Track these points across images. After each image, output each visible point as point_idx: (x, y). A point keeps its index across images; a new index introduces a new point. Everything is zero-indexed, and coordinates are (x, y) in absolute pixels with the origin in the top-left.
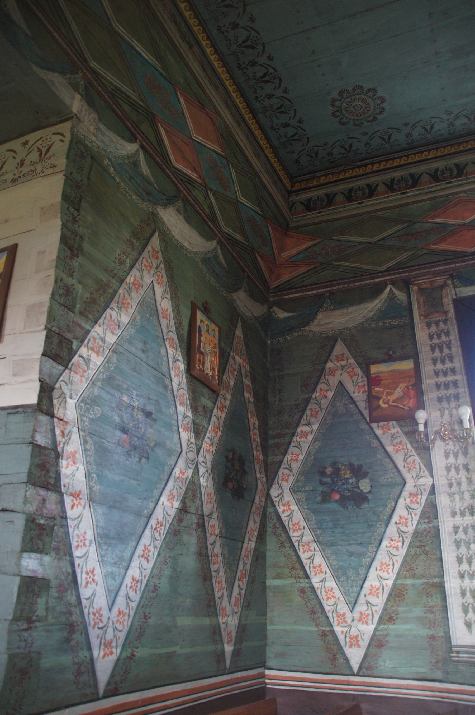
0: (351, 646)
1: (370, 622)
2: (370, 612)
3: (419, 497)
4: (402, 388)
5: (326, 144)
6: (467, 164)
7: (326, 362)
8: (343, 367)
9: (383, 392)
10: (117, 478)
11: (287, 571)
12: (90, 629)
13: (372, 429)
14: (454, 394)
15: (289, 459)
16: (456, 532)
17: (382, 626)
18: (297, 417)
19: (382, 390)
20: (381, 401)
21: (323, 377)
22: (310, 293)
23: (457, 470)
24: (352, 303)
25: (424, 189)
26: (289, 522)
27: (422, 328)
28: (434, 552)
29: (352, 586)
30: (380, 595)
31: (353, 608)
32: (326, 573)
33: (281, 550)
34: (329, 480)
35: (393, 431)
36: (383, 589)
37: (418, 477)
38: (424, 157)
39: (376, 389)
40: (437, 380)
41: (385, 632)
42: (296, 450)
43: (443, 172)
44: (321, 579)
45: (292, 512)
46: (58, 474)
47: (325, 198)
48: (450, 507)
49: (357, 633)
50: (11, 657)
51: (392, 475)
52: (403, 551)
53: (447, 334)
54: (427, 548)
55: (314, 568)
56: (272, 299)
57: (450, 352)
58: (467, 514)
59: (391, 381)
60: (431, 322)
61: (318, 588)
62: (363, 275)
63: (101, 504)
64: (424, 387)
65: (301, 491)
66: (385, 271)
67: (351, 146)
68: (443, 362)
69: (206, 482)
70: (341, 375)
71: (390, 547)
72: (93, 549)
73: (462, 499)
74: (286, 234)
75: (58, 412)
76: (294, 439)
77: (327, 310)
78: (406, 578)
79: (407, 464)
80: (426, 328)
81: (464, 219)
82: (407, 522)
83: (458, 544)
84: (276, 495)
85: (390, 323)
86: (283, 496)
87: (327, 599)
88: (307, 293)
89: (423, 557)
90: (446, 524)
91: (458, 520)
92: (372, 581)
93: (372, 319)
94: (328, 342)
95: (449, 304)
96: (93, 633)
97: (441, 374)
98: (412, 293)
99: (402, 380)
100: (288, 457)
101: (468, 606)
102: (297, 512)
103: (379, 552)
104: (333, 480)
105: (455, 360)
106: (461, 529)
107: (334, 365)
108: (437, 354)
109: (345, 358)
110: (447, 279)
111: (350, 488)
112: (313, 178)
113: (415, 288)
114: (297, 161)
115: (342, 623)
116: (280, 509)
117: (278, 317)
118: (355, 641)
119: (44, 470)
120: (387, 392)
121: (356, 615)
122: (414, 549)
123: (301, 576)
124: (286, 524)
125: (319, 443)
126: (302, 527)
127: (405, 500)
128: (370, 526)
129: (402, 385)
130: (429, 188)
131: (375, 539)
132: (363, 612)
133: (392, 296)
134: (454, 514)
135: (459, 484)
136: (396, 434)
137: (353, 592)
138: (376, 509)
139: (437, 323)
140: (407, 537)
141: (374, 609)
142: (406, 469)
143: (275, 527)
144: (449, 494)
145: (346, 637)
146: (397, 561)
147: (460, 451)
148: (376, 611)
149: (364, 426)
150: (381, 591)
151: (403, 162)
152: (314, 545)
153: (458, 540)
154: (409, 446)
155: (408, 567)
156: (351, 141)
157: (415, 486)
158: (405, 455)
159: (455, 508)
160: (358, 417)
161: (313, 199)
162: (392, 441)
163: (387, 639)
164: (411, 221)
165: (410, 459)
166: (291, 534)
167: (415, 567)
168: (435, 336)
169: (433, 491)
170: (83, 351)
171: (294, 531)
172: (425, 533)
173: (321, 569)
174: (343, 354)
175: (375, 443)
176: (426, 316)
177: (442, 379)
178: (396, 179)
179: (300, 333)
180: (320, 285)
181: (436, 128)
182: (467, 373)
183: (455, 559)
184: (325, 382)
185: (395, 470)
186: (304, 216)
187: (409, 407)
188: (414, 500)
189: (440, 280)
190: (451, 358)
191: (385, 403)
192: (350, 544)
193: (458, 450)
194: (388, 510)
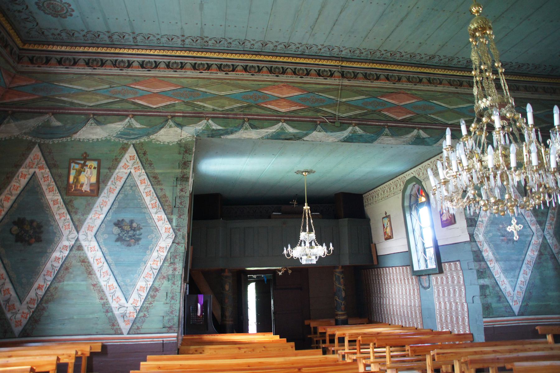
10: (505, 252)
12: (507, 297)
46: (483, 257)
50: (483, 304)
63: (500, 261)
69: (550, 241)
72: (502, 275)
75: (477, 240)
96: (509, 299)
119: (478, 257)
170: (480, 219)
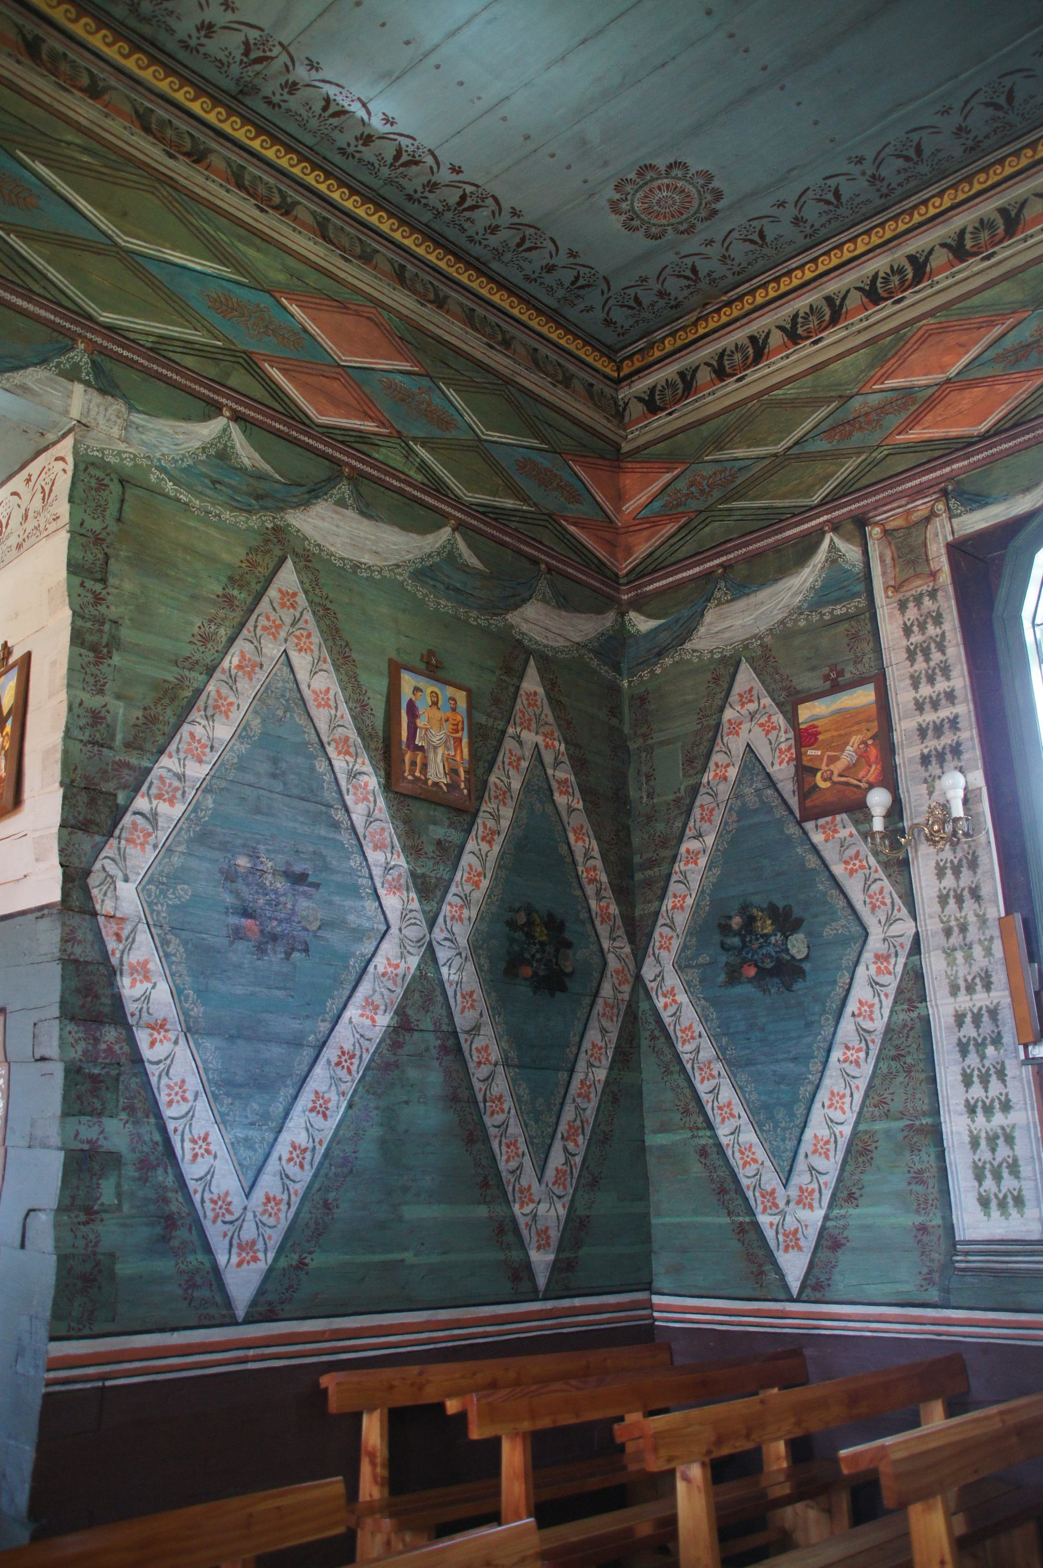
1: (816, 1204)
2: (815, 1186)
3: (892, 961)
5: (644, 280)
7: (721, 710)
8: (752, 716)
10: (239, 990)
11: (677, 1117)
12: (207, 1224)
13: (805, 833)
19: (819, 753)
20: (819, 775)
21: (719, 740)
22: (691, 572)
23: (960, 900)
27: (891, 616)
29: (783, 1140)
30: (831, 1154)
31: (787, 1180)
35: (843, 833)
36: (836, 1142)
37: (890, 921)
38: (847, 256)
41: (842, 1222)
43: (886, 280)
46: (118, 1000)
47: (679, 381)
49: (796, 1225)
51: (843, 922)
52: (868, 1069)
54: (909, 1060)
55: (720, 1108)
56: (625, 597)
57: (943, 658)
58: (979, 988)
60: (907, 600)
62: (781, 521)
63: (209, 1034)
64: (897, 737)
65: (693, 967)
68: (931, 680)
69: (457, 973)
71: (845, 1061)
72: (202, 1106)
73: (969, 959)
75: (105, 906)
76: (676, 868)
78: (873, 1119)
79: (870, 897)
80: (897, 613)
81: (943, 369)
82: (872, 1012)
83: (963, 1048)
85: (831, 613)
88: (684, 574)
90: (942, 1008)
91: (963, 1002)
92: (816, 1128)
93: (799, 610)
96: (215, 1232)
97: (927, 707)
99: (856, 728)
100: (669, 903)
101: (984, 1168)
103: (827, 1073)
104: (743, 941)
105: (955, 673)
106: (968, 1019)
109: (755, 698)
110: (937, 500)
112: (651, 346)
113: (877, 530)
114: (608, 322)
116: (660, 1003)
118: (793, 1240)
119: (91, 997)
121: (793, 1192)
124: (671, 1029)
126: (696, 1034)
128: (809, 1025)
129: (856, 739)
131: (819, 1048)
133: (834, 557)
134: (954, 990)
135: (963, 928)
137: (786, 1150)
139: (918, 600)
140: (873, 1041)
141: (822, 1179)
142: (869, 906)
143: (653, 1038)
144: (944, 952)
145: (777, 1233)
146: (857, 1087)
148: (825, 1184)
150: (832, 1146)
151: (809, 275)
152: (718, 1067)
155: (877, 1098)
157: (885, 940)
158: (866, 880)
159: (956, 977)
164: (840, 397)
165: (875, 887)
166: (679, 1048)
168: (915, 628)
170: (141, 803)
174: (751, 690)
175: (812, 862)
176: (896, 589)
181: (846, 193)
183: (960, 1078)
189: (921, 506)
191: (825, 780)
192: (777, 1061)
193: (960, 860)
194: (840, 991)
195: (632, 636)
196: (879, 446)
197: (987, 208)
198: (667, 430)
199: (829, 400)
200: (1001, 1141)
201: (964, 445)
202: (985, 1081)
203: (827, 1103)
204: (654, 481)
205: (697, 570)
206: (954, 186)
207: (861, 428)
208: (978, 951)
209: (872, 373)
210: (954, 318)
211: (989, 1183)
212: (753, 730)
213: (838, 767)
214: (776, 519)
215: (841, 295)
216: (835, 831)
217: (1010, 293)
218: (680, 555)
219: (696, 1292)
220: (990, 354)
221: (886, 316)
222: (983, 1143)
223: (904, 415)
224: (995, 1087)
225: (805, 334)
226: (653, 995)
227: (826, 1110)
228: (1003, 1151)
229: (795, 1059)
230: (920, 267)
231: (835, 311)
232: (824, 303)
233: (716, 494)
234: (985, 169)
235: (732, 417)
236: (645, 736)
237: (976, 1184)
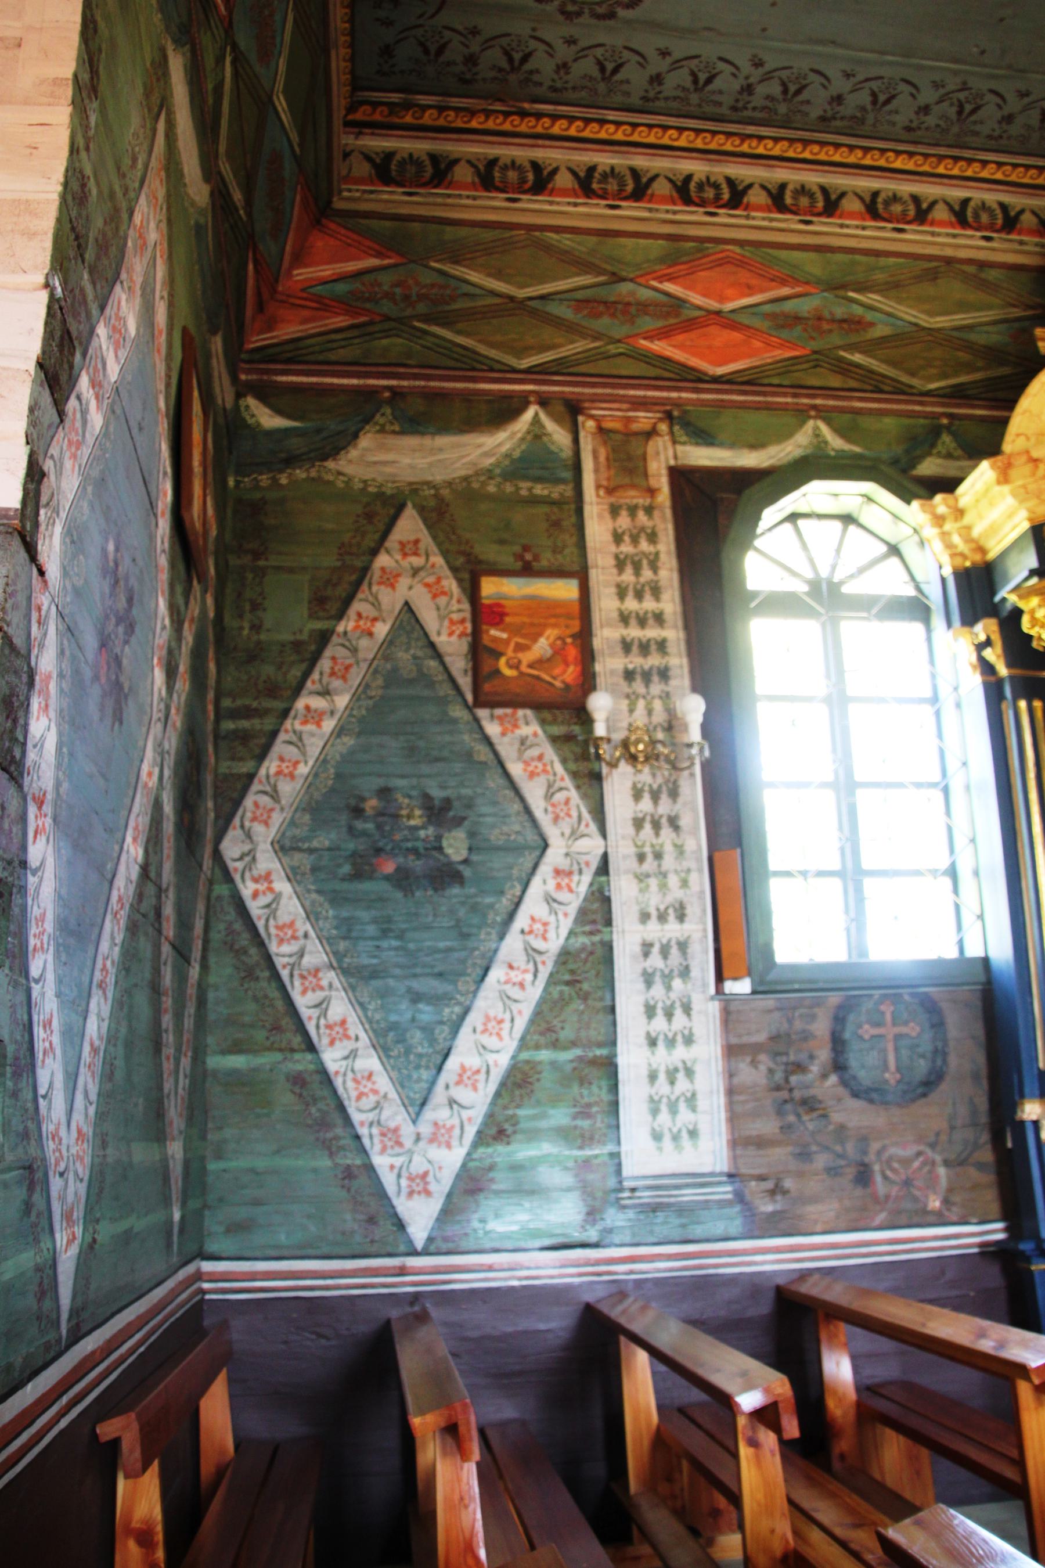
0: (411, 1194)
1: (455, 1142)
2: (456, 1122)
3: (576, 878)
4: (552, 639)
5: (475, 32)
6: (750, 186)
7: (374, 552)
8: (415, 572)
9: (507, 642)
11: (260, 1035)
13: (477, 720)
14: (658, 668)
15: (273, 770)
16: (646, 955)
17: (481, 1150)
18: (296, 672)
19: (505, 636)
20: (503, 661)
21: (365, 586)
22: (345, 381)
23: (656, 826)
24: (445, 427)
25: (657, 210)
26: (267, 920)
27: (600, 516)
28: (600, 993)
29: (418, 1067)
30: (481, 1086)
31: (418, 1114)
32: (357, 1039)
33: (246, 986)
34: (370, 826)
35: (525, 730)
36: (488, 1072)
37: (575, 835)
38: (666, 141)
39: (493, 632)
40: (624, 632)
41: (488, 1161)
42: (292, 752)
43: (700, 186)
44: (346, 1053)
45: (278, 897)
47: (427, 163)
48: (638, 903)
49: (426, 1166)
51: (517, 827)
52: (535, 992)
53: (653, 537)
54: (585, 986)
55: (329, 1027)
56: (243, 377)
59: (526, 620)
60: (620, 507)
61: (337, 1073)
62: (474, 369)
64: (597, 643)
65: (299, 850)
66: (528, 371)
67: (526, 58)
68: (639, 596)
70: (410, 588)
71: (506, 982)
73: (663, 887)
74: (318, 222)
76: (288, 724)
77: (382, 431)
78: (537, 1047)
79: (553, 805)
81: (722, 299)
82: (546, 931)
83: (648, 979)
84: (237, 855)
85: (530, 489)
86: (254, 859)
87: (359, 1098)
88: (335, 381)
89: (578, 1005)
90: (627, 937)
91: (653, 931)
92: (464, 1054)
93: (489, 473)
94: (383, 508)
95: (659, 475)
97: (633, 622)
98: (582, 434)
99: (553, 621)
100: (271, 766)
101: (660, 1101)
102: (290, 898)
103: (482, 994)
104: (379, 827)
105: (666, 596)
106: (656, 950)
107: (393, 564)
108: (628, 576)
109: (422, 551)
110: (661, 420)
111: (422, 851)
112: (407, 106)
113: (591, 424)
114: (387, 51)
115: (392, 1147)
116: (247, 889)
117: (259, 424)
118: (420, 1184)
120: (517, 645)
121: (425, 1129)
122: (559, 988)
123: (296, 1047)
124: (260, 925)
125: (349, 741)
126: (300, 933)
127: (545, 882)
128: (465, 936)
129: (552, 633)
130: (667, 211)
132: (441, 1123)
133: (537, 433)
134: (645, 917)
135: (658, 856)
136: (531, 738)
137: (419, 1080)
138: (479, 900)
139: (633, 510)
140: (544, 963)
141: (465, 1114)
142: (550, 816)
143: (230, 931)
144: (636, 876)
145: (399, 1176)
146: (520, 1012)
147: (664, 788)
148: (470, 1119)
149: (458, 712)
150: (482, 1077)
151: (619, 136)
152: (330, 977)
153: (650, 970)
154: (559, 768)
155: (544, 1026)
156: (533, 44)
157: (567, 855)
158: (550, 786)
159: (647, 905)
160: (446, 690)
161: (398, 157)
162: (521, 752)
163: (491, 1175)
164: (614, 274)
165: (560, 797)
166: (273, 948)
167: (559, 1025)
168: (626, 538)
169: (604, 867)
171: (281, 941)
172: (583, 956)
173: (346, 1030)
174: (417, 542)
175: (482, 753)
176: (610, 491)
177: (634, 632)
178: (600, 169)
179: (313, 473)
180: (368, 369)
181: (717, 84)
182: (686, 627)
183: (642, 1009)
184: (371, 598)
185: (526, 817)
186: (372, 192)
187: (563, 682)
188: (563, 884)
189: (644, 419)
190: (656, 592)
191: (511, 667)
192: (415, 976)
193: (660, 786)
194: (505, 902)
195: (248, 426)
196: (619, 341)
197: (813, 178)
198: (404, 211)
199: (601, 272)
200: (681, 1076)
201: (696, 379)
202: (669, 1015)
203: (480, 1028)
204: (358, 259)
205: (355, 381)
206: (792, 141)
207: (613, 315)
208: (673, 881)
209: (657, 267)
210: (755, 261)
211: (664, 1117)
212: (412, 587)
213: (526, 657)
214: (472, 365)
215: (649, 175)
216: (516, 726)
217: (812, 264)
218: (332, 356)
219: (326, 1250)
220: (767, 308)
221: (692, 220)
222: (662, 1077)
223: (660, 324)
224: (679, 1020)
225: (600, 192)
226: (237, 878)
227: (478, 1036)
228: (682, 1084)
229: (440, 975)
230: (737, 196)
231: (640, 188)
232: (628, 173)
233: (421, 308)
234: (822, 144)
235: (488, 235)
236: (257, 555)
237: (650, 1118)
